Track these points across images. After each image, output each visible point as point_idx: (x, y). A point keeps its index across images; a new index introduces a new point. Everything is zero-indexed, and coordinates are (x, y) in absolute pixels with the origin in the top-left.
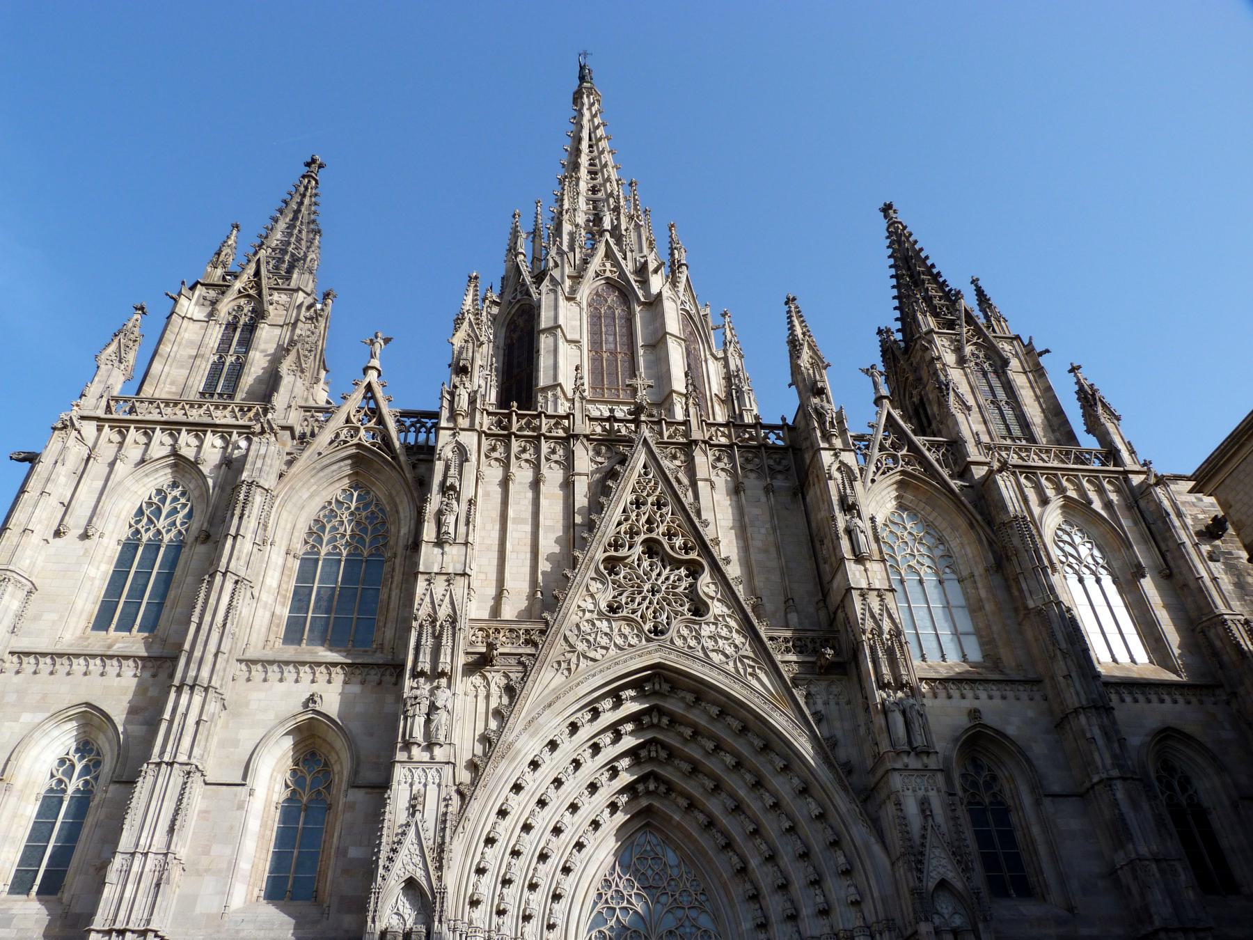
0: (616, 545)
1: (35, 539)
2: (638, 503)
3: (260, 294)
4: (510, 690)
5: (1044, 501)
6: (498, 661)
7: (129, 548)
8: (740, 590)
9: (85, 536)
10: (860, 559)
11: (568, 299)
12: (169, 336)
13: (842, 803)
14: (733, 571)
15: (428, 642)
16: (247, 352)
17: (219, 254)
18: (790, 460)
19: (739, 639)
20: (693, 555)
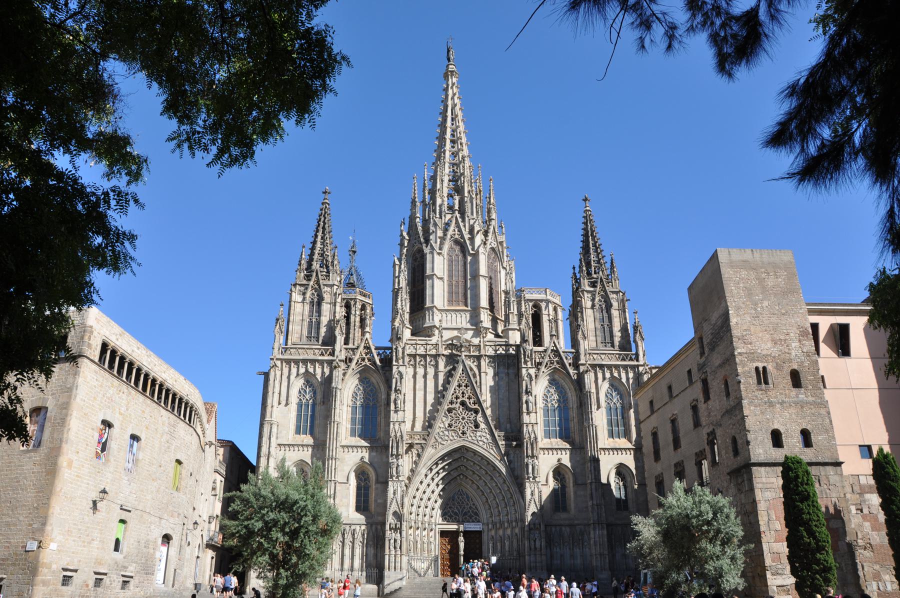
0: (452, 403)
1: (275, 408)
2: (459, 386)
3: (320, 287)
4: (419, 455)
5: (604, 379)
6: (415, 446)
7: (300, 405)
8: (490, 419)
9: (287, 404)
10: (528, 413)
11: (439, 254)
12: (292, 312)
13: (513, 489)
14: (488, 412)
15: (395, 445)
16: (319, 316)
17: (300, 265)
18: (515, 361)
19: (488, 436)
20: (476, 406)
